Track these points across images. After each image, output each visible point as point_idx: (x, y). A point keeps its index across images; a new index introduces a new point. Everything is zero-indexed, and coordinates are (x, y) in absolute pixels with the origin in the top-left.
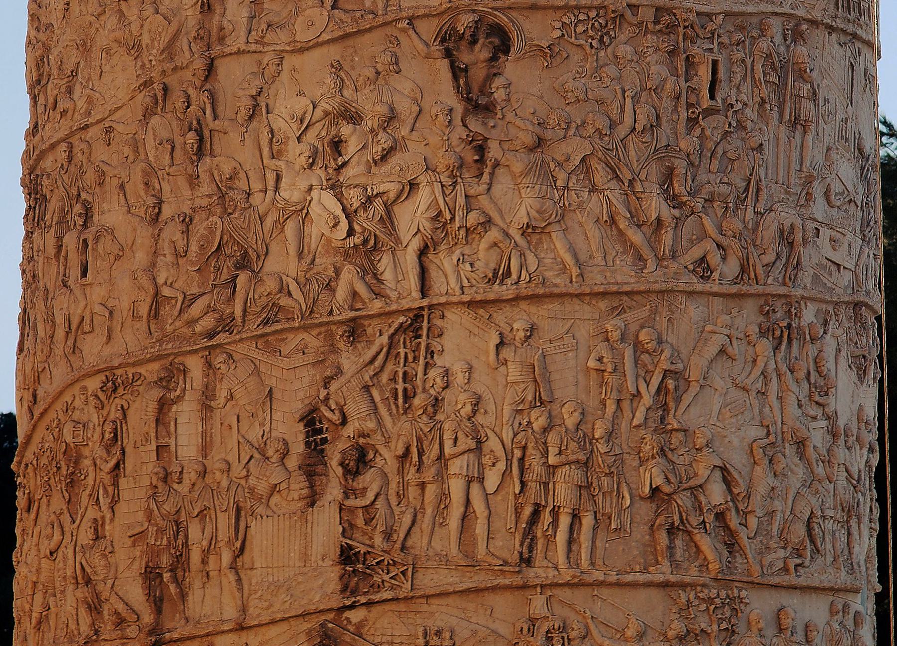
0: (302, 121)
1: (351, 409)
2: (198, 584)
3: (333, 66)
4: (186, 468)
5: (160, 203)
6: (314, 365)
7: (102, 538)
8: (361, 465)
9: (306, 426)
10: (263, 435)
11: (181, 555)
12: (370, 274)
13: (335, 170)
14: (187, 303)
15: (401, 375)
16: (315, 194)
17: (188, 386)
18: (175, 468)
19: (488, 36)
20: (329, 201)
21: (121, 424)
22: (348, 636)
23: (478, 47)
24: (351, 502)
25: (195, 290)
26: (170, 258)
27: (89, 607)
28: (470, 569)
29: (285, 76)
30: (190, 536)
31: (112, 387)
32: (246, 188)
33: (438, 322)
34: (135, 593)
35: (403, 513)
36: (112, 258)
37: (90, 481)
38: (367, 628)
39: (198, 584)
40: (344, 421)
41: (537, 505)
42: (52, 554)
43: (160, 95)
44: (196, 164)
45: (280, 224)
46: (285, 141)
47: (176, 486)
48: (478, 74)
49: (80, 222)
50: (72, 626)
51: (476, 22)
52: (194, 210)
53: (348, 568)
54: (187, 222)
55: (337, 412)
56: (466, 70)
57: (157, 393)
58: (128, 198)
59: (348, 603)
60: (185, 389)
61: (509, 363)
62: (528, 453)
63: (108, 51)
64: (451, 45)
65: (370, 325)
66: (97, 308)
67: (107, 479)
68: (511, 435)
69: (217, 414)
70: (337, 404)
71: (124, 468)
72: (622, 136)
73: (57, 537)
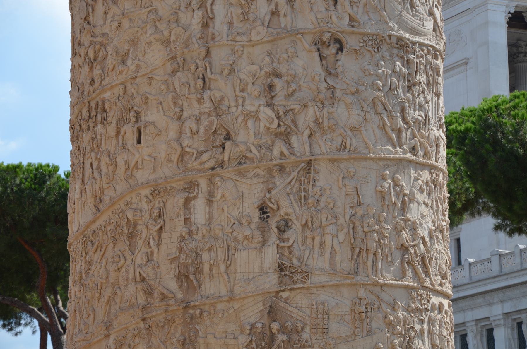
0: (255, 76)
1: (282, 203)
2: (207, 280)
3: (268, 53)
4: (200, 228)
5: (182, 111)
6: (263, 183)
7: (151, 260)
8: (286, 228)
9: (260, 210)
10: (239, 214)
11: (199, 267)
12: (288, 143)
13: (271, 98)
14: (198, 155)
15: (302, 189)
16: (262, 108)
17: (200, 191)
18: (194, 228)
19: (334, 43)
20: (269, 112)
21: (163, 208)
22: (282, 304)
23: (331, 47)
24: (282, 244)
25: (202, 149)
26: (189, 135)
27: (145, 291)
28: (334, 275)
29: (245, 56)
30: (203, 259)
31: (156, 192)
32: (228, 105)
33: (316, 166)
34: (173, 284)
35: (305, 250)
36: (154, 135)
37: (144, 235)
38: (290, 300)
39: (207, 280)
40: (278, 208)
41: (360, 248)
42: (118, 269)
43: (181, 64)
44: (202, 93)
45: (245, 121)
46: (247, 84)
47: (194, 236)
48: (331, 59)
49: (134, 119)
50: (133, 300)
51: (330, 37)
52: (200, 114)
53: (282, 273)
54: (198, 120)
55: (275, 204)
56: (326, 58)
57: (185, 195)
58: (164, 108)
59: (282, 289)
60: (198, 193)
61: (347, 186)
62: (355, 226)
63: (150, 43)
64: (319, 46)
65: (288, 167)
66: (146, 158)
67: (155, 234)
68: (349, 218)
69: (216, 205)
70: (275, 200)
71: (165, 229)
72: (386, 91)
73: (122, 261)
